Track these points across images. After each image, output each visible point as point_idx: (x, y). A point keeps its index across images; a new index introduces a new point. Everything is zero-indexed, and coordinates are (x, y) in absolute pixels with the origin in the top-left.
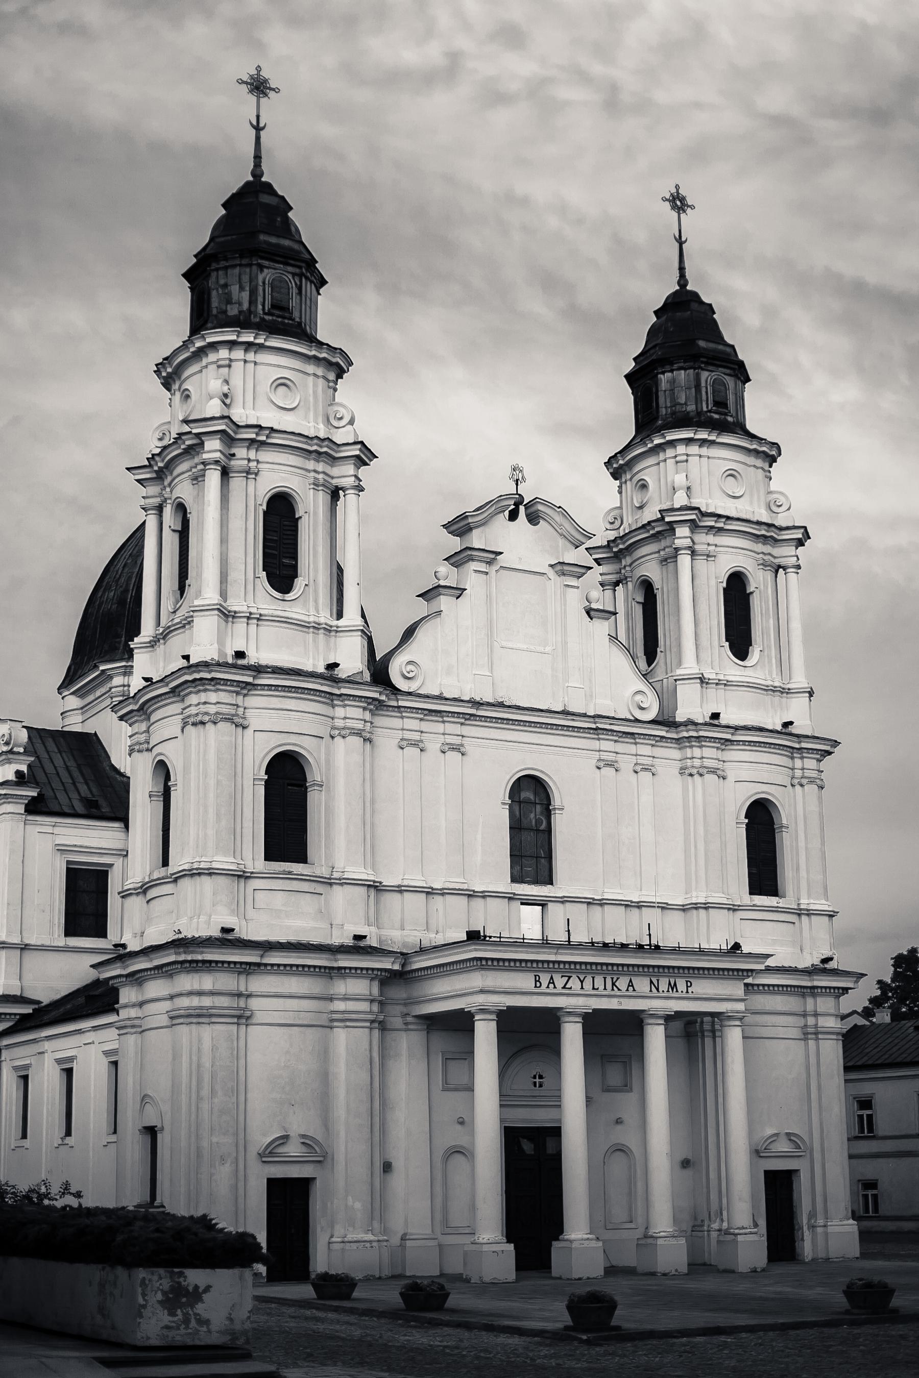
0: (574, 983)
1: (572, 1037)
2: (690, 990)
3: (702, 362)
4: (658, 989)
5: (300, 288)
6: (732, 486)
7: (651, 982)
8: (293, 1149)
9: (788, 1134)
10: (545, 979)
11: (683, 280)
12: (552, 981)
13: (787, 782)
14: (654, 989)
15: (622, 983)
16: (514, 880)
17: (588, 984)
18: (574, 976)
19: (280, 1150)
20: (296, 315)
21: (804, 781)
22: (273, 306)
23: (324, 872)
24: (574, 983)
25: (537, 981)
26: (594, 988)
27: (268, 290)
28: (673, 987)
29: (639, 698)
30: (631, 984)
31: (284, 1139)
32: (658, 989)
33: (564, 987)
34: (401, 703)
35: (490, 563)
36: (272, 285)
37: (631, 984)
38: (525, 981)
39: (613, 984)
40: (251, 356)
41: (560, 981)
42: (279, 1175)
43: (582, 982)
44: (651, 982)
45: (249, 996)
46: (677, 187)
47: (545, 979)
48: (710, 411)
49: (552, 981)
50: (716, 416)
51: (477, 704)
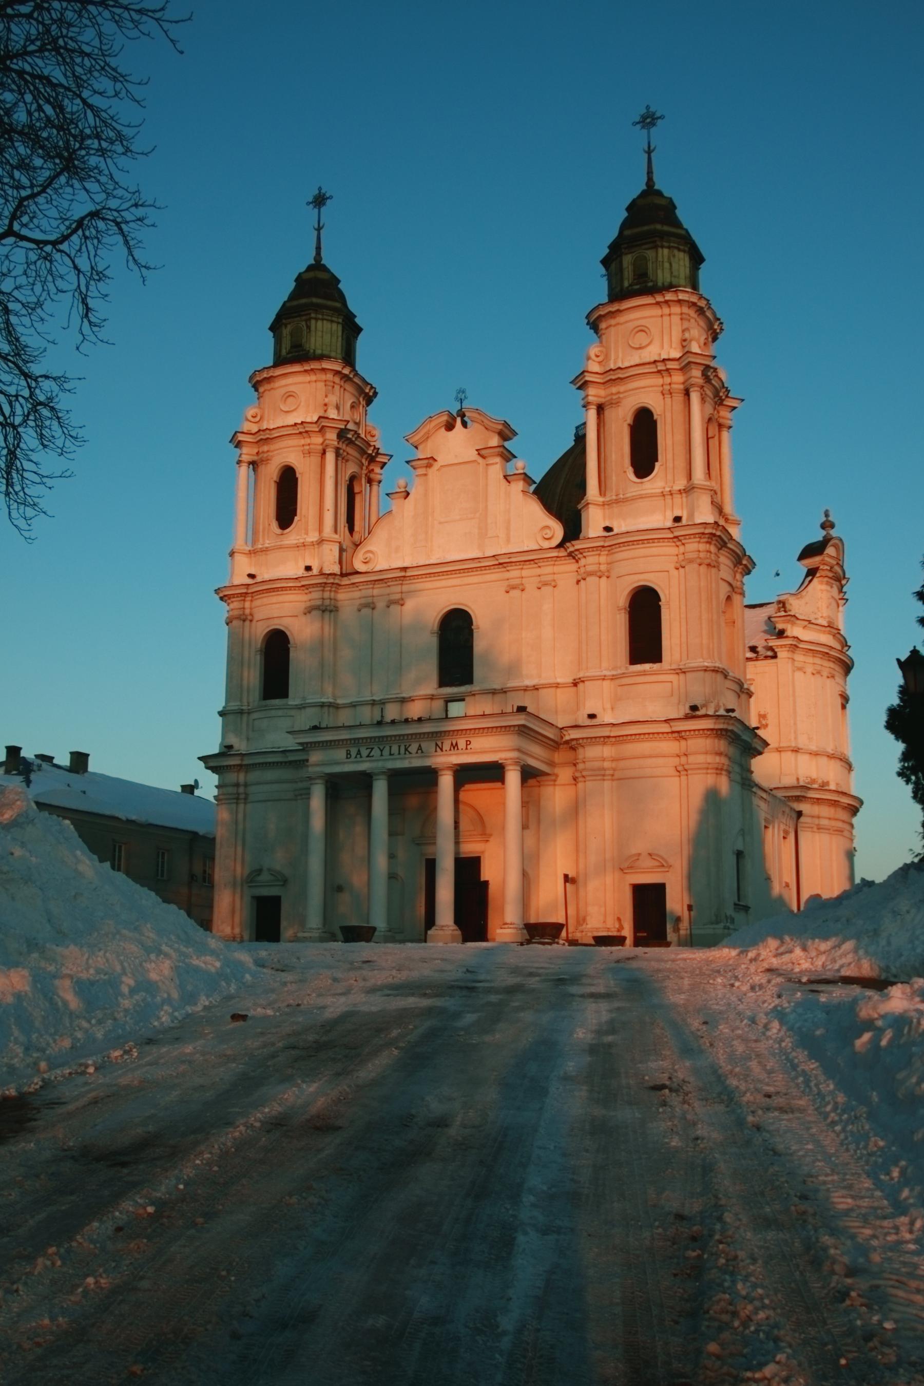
0: (376, 752)
1: (380, 789)
2: (469, 747)
3: (625, 248)
4: (442, 750)
5: (309, 327)
6: (641, 339)
7: (437, 745)
8: (265, 877)
9: (650, 855)
10: (354, 752)
11: (650, 182)
12: (359, 753)
13: (671, 567)
14: (438, 749)
15: (414, 748)
16: (442, 684)
17: (386, 752)
18: (376, 748)
19: (259, 878)
20: (307, 347)
21: (683, 564)
22: (292, 347)
23: (297, 702)
24: (376, 752)
25: (348, 754)
26: (391, 754)
27: (289, 337)
28: (455, 746)
29: (548, 531)
30: (420, 748)
31: (259, 871)
32: (442, 750)
33: (368, 756)
34: (353, 581)
35: (429, 466)
36: (291, 334)
37: (420, 748)
38: (341, 754)
39: (406, 749)
40: (272, 385)
41: (365, 752)
42: (258, 894)
43: (382, 751)
44: (437, 745)
45: (246, 785)
46: (648, 107)
47: (354, 752)
48: (631, 285)
49: (359, 753)
50: (637, 287)
51: (405, 569)
